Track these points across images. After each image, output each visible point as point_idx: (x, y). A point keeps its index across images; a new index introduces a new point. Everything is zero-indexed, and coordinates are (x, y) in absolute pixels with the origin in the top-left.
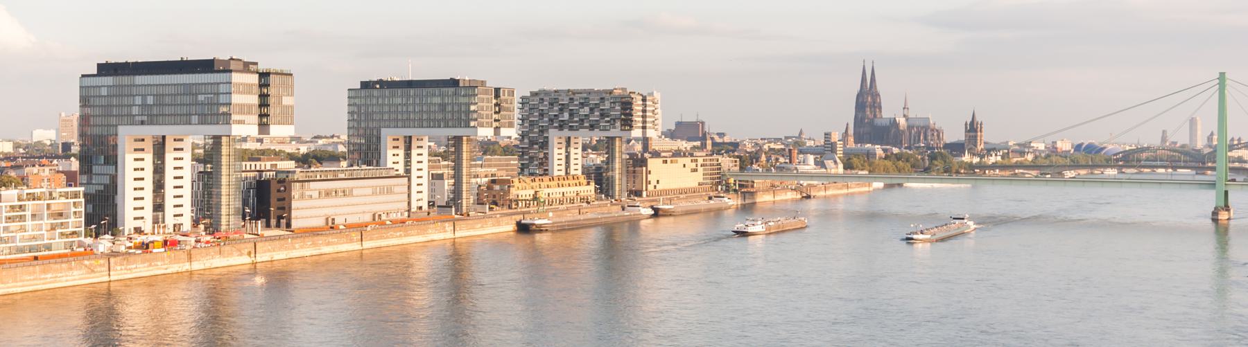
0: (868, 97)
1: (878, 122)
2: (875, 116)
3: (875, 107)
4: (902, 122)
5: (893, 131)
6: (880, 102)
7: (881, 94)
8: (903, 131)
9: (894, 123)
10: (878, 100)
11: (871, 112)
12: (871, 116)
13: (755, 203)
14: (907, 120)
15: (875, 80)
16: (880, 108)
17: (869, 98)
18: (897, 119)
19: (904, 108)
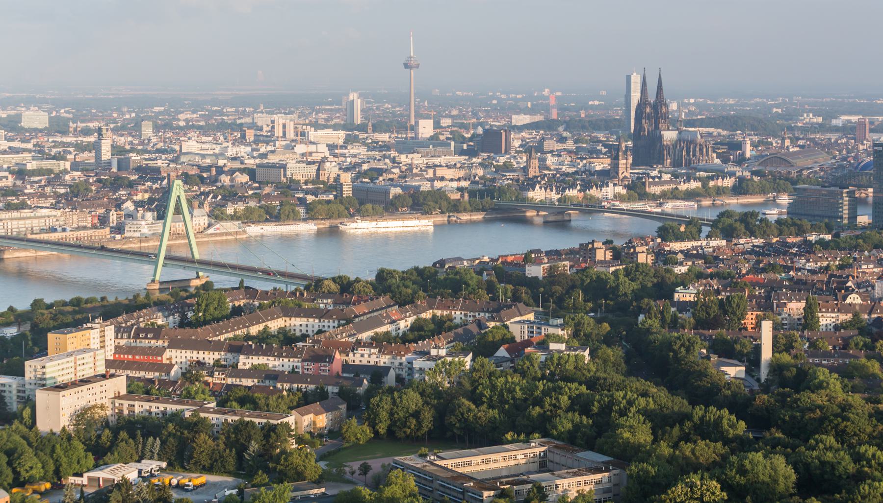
13: (3, 259)
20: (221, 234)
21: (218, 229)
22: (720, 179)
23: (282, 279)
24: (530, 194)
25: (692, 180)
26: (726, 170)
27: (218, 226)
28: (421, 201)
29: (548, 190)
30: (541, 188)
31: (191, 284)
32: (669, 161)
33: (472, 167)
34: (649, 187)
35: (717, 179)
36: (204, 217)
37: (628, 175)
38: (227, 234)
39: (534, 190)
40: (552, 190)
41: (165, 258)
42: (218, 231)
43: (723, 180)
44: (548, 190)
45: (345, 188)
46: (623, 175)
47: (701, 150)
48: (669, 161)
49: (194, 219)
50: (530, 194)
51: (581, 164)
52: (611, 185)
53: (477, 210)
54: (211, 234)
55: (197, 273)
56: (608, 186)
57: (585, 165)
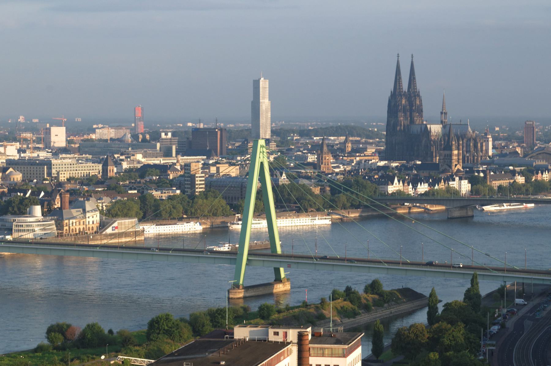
0: (401, 98)
1: (415, 129)
2: (412, 122)
3: (411, 111)
4: (436, 129)
5: (423, 142)
6: (421, 105)
7: (421, 94)
8: (434, 141)
9: (427, 132)
10: (418, 102)
11: (406, 118)
12: (407, 122)
14: (444, 127)
15: (414, 78)
16: (420, 111)
17: (404, 102)
18: (428, 126)
19: (442, 113)
20: (120, 235)
21: (117, 228)
22: (540, 175)
23: (500, 274)
24: (391, 189)
25: (517, 175)
26: (534, 164)
27: (115, 224)
28: (287, 196)
29: (406, 184)
30: (399, 181)
31: (275, 291)
32: (438, 158)
33: (246, 165)
34: (490, 181)
35: (537, 173)
36: (97, 213)
37: (460, 168)
38: (126, 234)
39: (393, 184)
40: (409, 185)
41: (249, 254)
42: (116, 231)
43: (542, 174)
44: (406, 184)
45: (198, 181)
46: (456, 168)
47: (475, 146)
48: (438, 158)
49: (88, 215)
50: (391, 189)
51: (355, 162)
52: (457, 179)
53: (354, 207)
54: (111, 235)
55: (277, 271)
56: (454, 180)
57: (359, 163)
